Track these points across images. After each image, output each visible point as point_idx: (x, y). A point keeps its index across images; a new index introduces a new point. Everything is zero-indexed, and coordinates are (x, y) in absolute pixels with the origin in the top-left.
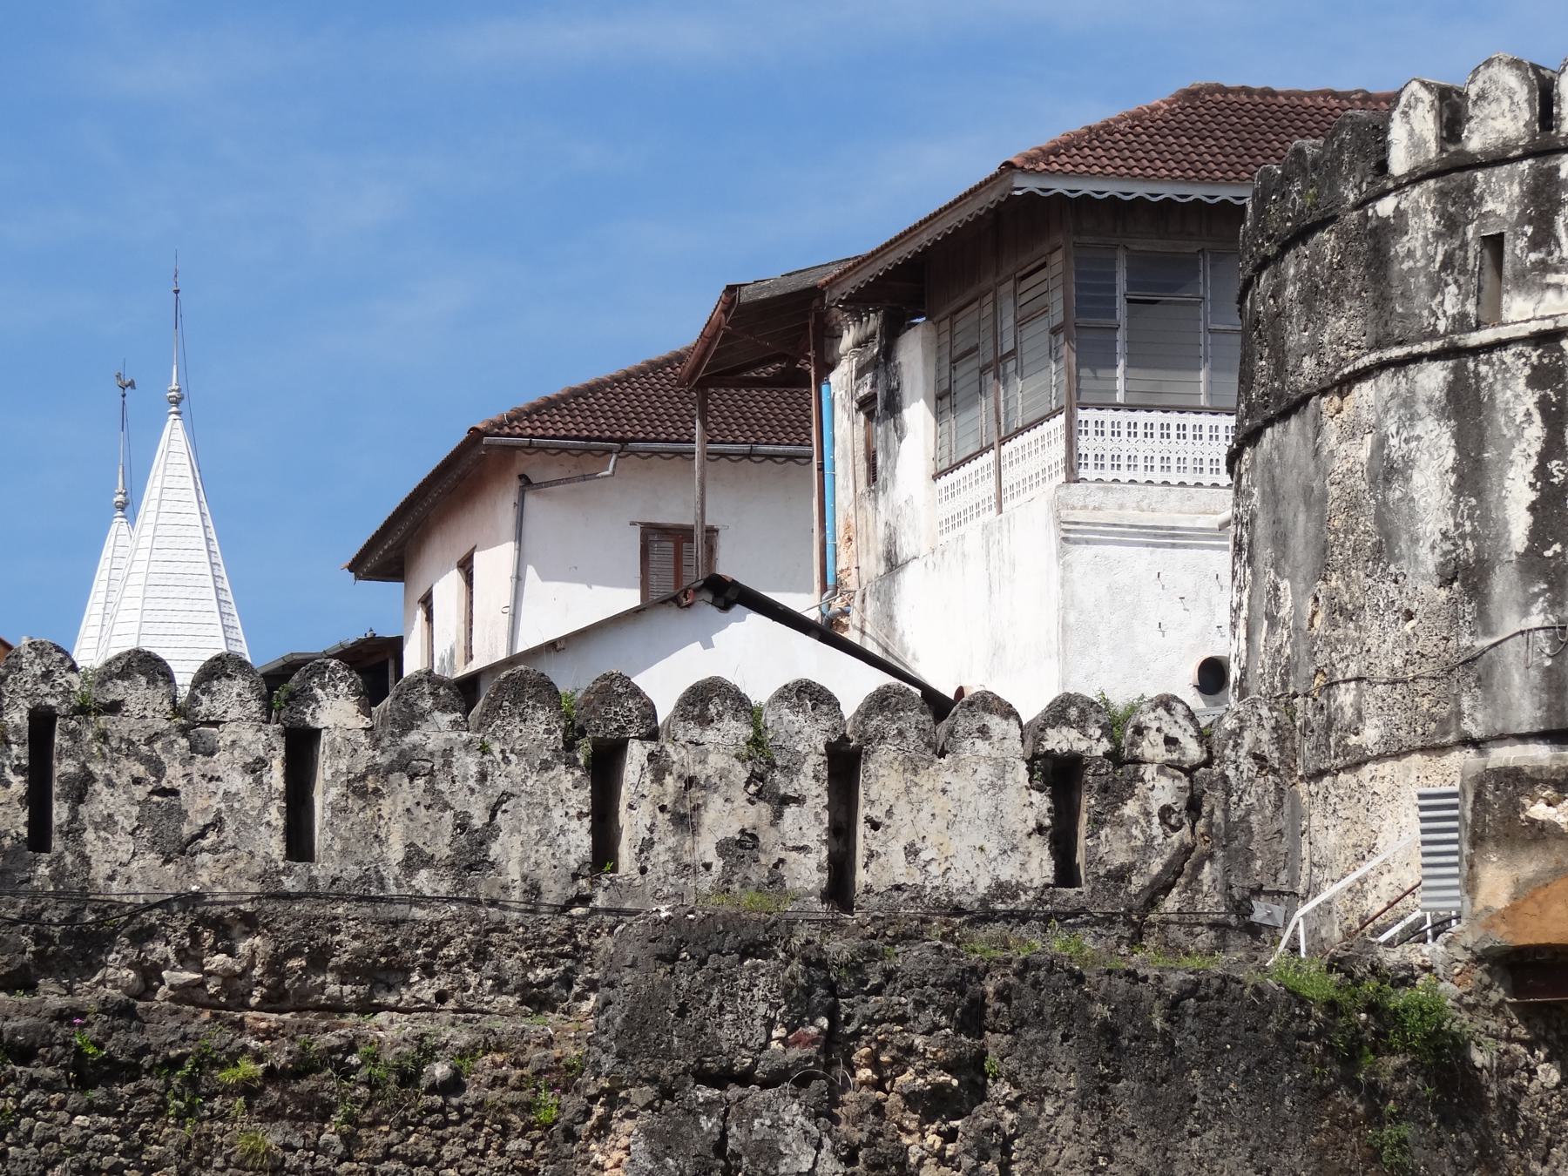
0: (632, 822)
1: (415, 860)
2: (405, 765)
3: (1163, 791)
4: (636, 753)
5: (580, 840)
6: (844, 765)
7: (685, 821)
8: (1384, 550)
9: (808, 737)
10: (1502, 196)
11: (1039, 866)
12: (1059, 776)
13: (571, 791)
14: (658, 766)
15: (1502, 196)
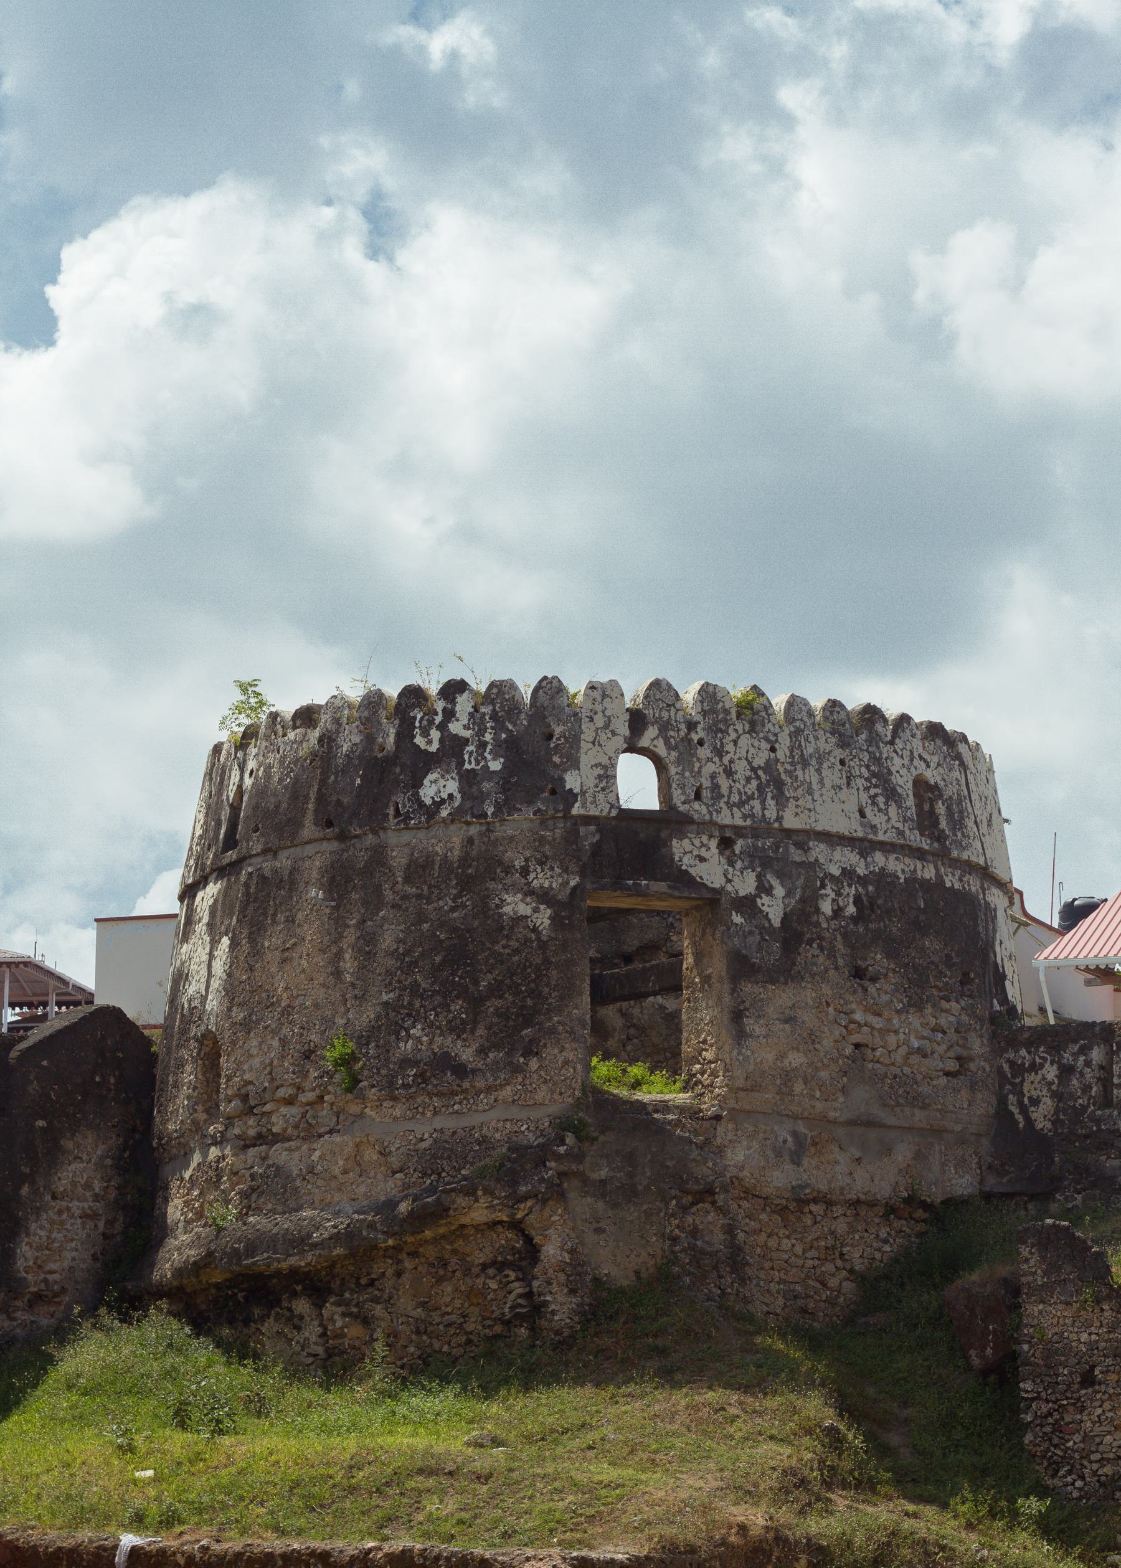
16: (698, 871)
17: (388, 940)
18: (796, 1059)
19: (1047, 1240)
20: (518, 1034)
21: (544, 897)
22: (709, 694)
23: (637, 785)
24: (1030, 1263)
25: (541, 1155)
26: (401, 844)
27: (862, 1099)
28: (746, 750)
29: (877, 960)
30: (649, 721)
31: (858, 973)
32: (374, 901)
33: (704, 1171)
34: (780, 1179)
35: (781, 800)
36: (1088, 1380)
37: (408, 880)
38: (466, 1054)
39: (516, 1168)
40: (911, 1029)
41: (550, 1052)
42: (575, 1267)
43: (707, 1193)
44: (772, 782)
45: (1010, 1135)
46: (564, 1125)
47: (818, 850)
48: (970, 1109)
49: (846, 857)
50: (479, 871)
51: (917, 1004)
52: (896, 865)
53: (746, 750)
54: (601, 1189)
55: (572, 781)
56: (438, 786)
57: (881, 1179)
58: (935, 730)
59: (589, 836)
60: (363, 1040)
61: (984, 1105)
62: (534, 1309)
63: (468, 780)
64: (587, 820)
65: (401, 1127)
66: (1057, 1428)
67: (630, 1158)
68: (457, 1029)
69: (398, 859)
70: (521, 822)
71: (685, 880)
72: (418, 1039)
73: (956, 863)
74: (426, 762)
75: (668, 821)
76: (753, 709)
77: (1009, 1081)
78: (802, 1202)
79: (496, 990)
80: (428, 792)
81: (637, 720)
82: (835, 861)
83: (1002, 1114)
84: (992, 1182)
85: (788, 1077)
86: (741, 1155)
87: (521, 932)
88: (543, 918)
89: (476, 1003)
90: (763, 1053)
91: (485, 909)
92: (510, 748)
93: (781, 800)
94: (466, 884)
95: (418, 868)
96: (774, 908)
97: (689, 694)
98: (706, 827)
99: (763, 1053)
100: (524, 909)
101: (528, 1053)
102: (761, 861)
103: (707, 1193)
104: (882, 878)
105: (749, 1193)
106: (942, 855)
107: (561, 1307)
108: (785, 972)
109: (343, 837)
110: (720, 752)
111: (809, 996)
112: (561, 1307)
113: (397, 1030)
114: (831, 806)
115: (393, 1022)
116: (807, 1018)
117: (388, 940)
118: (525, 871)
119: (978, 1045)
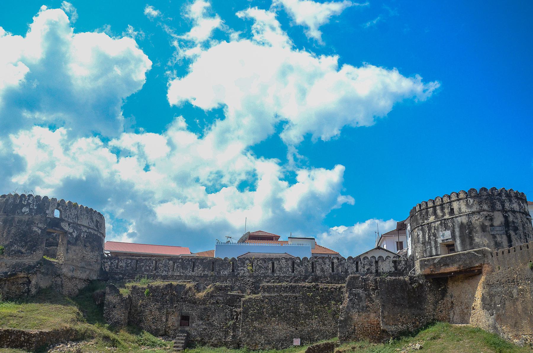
0: (359, 268)
1: (341, 272)
2: (341, 264)
3: (403, 263)
4: (359, 262)
5: (355, 269)
6: (377, 262)
7: (364, 268)
8: (418, 242)
9: (374, 261)
10: (424, 212)
11: (393, 269)
12: (395, 262)
13: (354, 266)
14: (361, 263)
15: (424, 212)
16: (65, 228)
17: (13, 232)
18: (75, 257)
19: (111, 287)
20: (33, 248)
21: (40, 228)
22: (70, 202)
23: (57, 214)
24: (108, 290)
25: (34, 267)
26: (17, 217)
27: (83, 264)
28: (74, 212)
29: (88, 244)
30: (60, 205)
31: (85, 246)
32: (11, 225)
33: (59, 272)
34: (70, 274)
35: (78, 220)
36: (114, 307)
37: (18, 223)
38: (23, 250)
39: (29, 269)
40: (91, 255)
41: (38, 252)
42: (37, 286)
43: (59, 275)
44: (77, 217)
45: (102, 272)
46: (38, 263)
47: (82, 227)
48: (97, 267)
49: (86, 229)
50: (30, 223)
51: (92, 251)
52: (92, 231)
53: (74, 212)
54: (43, 273)
55: (47, 212)
56: (25, 210)
57: (84, 276)
58: (99, 213)
59: (49, 220)
60: (5, 247)
61: (99, 267)
62: (29, 291)
63: (30, 209)
64: (49, 218)
65: (10, 261)
66: (109, 314)
67: (48, 269)
68: (22, 246)
69: (16, 220)
70: (38, 217)
71: (62, 229)
72: (15, 247)
73: (100, 232)
74: (25, 206)
75: (61, 220)
76: (76, 206)
77: (103, 264)
78: (72, 278)
79: (29, 241)
80: (23, 210)
81: (59, 205)
82: (84, 229)
83: (101, 269)
84: (99, 278)
85: (73, 259)
86: (65, 270)
87: (35, 233)
88: (40, 231)
89: (26, 243)
90: (70, 256)
91: (30, 229)
92: (38, 206)
93: (78, 220)
94: (27, 225)
95: (20, 221)
96: (75, 235)
97: (67, 202)
98: (67, 221)
99: (70, 256)
100: (36, 230)
101: (34, 251)
102: (74, 228)
103: (59, 275)
104: (90, 233)
105: (65, 276)
106: (98, 231)
107: (33, 291)
108: (75, 244)
109: (7, 215)
110: (70, 211)
111: (78, 248)
112: (33, 291)
113: (12, 245)
114: (84, 221)
115: (11, 244)
116: (77, 251)
117: (13, 232)
118: (38, 224)
119: (99, 258)
